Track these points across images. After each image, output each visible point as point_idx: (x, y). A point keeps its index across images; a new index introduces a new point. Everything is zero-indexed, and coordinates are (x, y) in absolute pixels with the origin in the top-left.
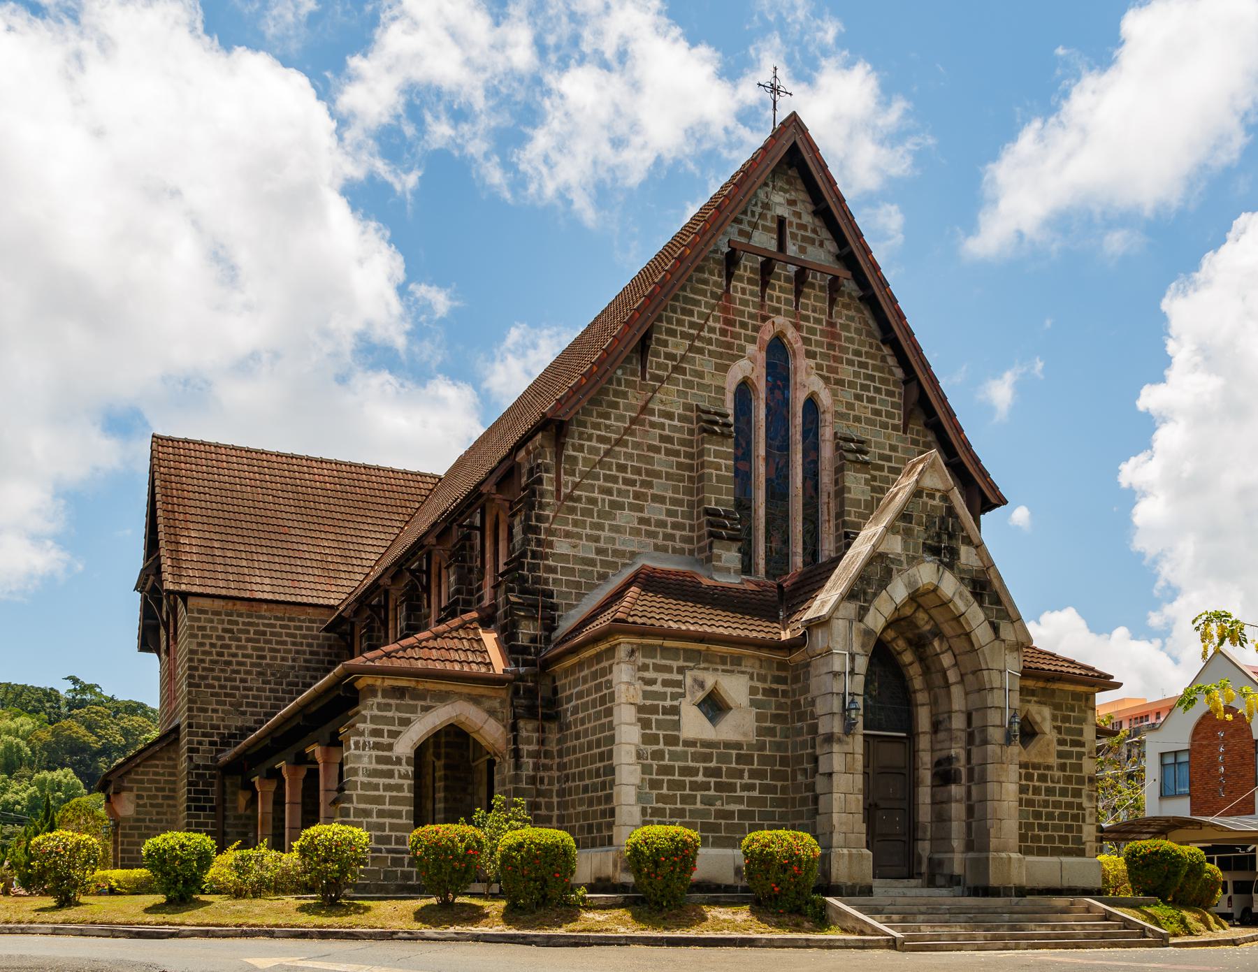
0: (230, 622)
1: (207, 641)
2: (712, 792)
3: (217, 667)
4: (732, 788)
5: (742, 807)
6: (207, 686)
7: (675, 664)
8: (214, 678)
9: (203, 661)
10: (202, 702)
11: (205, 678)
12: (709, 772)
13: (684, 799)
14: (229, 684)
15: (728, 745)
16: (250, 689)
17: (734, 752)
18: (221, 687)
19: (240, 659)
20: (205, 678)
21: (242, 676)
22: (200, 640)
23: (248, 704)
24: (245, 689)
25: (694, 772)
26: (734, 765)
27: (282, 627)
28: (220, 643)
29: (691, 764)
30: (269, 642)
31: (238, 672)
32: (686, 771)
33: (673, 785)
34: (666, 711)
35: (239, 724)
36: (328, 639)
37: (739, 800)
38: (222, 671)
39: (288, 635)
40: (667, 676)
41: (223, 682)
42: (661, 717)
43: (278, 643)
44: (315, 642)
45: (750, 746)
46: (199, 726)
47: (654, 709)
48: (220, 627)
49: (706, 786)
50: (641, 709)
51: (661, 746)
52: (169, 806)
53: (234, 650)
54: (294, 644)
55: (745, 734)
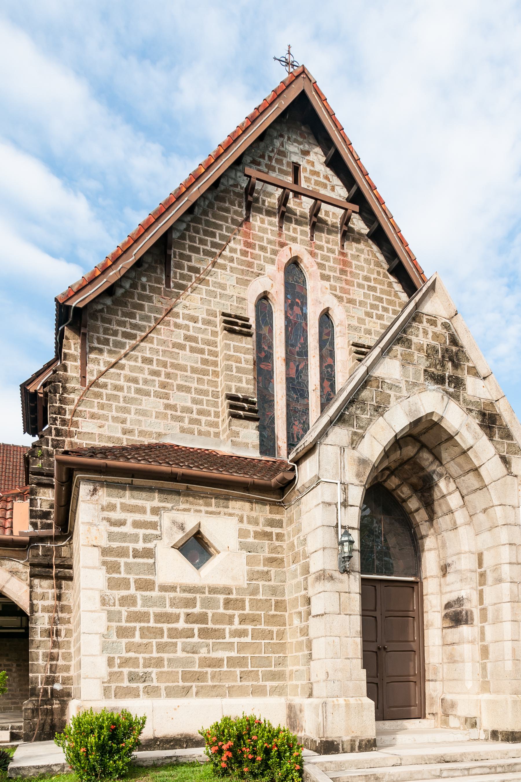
4: (219, 634)
13: (161, 647)
15: (213, 590)
17: (222, 597)
29: (169, 610)
32: (161, 617)
40: (138, 517)
42: (131, 560)
45: (239, 590)
47: (122, 553)
50: (105, 552)
51: (132, 591)
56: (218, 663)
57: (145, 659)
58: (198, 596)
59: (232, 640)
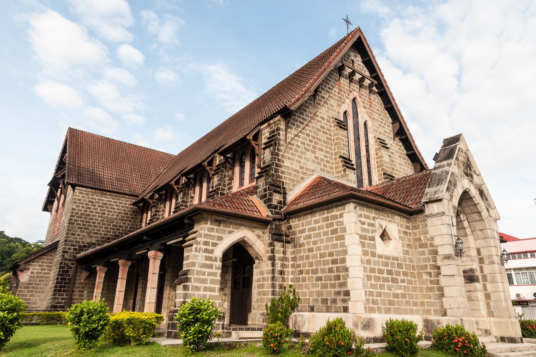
0: (92, 198)
1: (81, 205)
3: (83, 217)
6: (77, 224)
8: (81, 221)
9: (77, 213)
10: (73, 231)
11: (77, 220)
14: (87, 224)
16: (96, 227)
18: (83, 225)
19: (94, 214)
20: (77, 220)
21: (94, 221)
22: (78, 205)
23: (94, 233)
24: (94, 226)
27: (114, 202)
28: (86, 206)
30: (108, 208)
31: (92, 219)
35: (89, 241)
36: (133, 208)
38: (85, 218)
39: (116, 205)
41: (84, 223)
43: (111, 208)
44: (127, 209)
46: (70, 241)
48: (87, 200)
52: (46, 277)
53: (92, 210)
54: (118, 209)
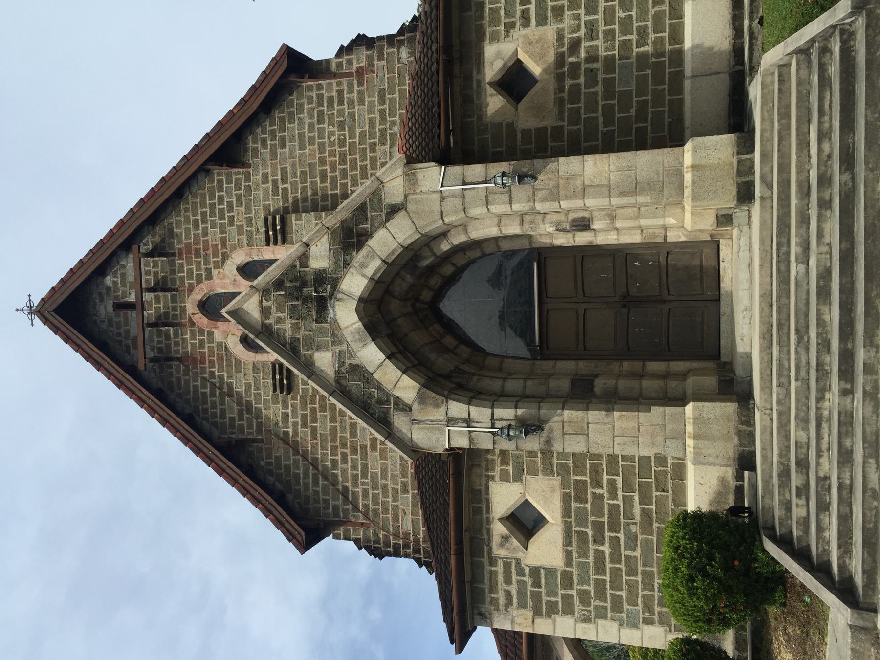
2: (622, 536)
5: (636, 497)
7: (487, 568)
12: (599, 539)
13: (632, 571)
15: (566, 512)
17: (574, 505)
25: (599, 554)
26: (588, 506)
29: (591, 560)
32: (600, 567)
33: (616, 584)
34: (536, 584)
37: (628, 501)
45: (565, 485)
47: (536, 597)
49: (615, 542)
50: (537, 613)
51: (574, 592)
55: (553, 490)
56: (646, 514)
57: (644, 589)
58: (574, 529)
59: (621, 497)
